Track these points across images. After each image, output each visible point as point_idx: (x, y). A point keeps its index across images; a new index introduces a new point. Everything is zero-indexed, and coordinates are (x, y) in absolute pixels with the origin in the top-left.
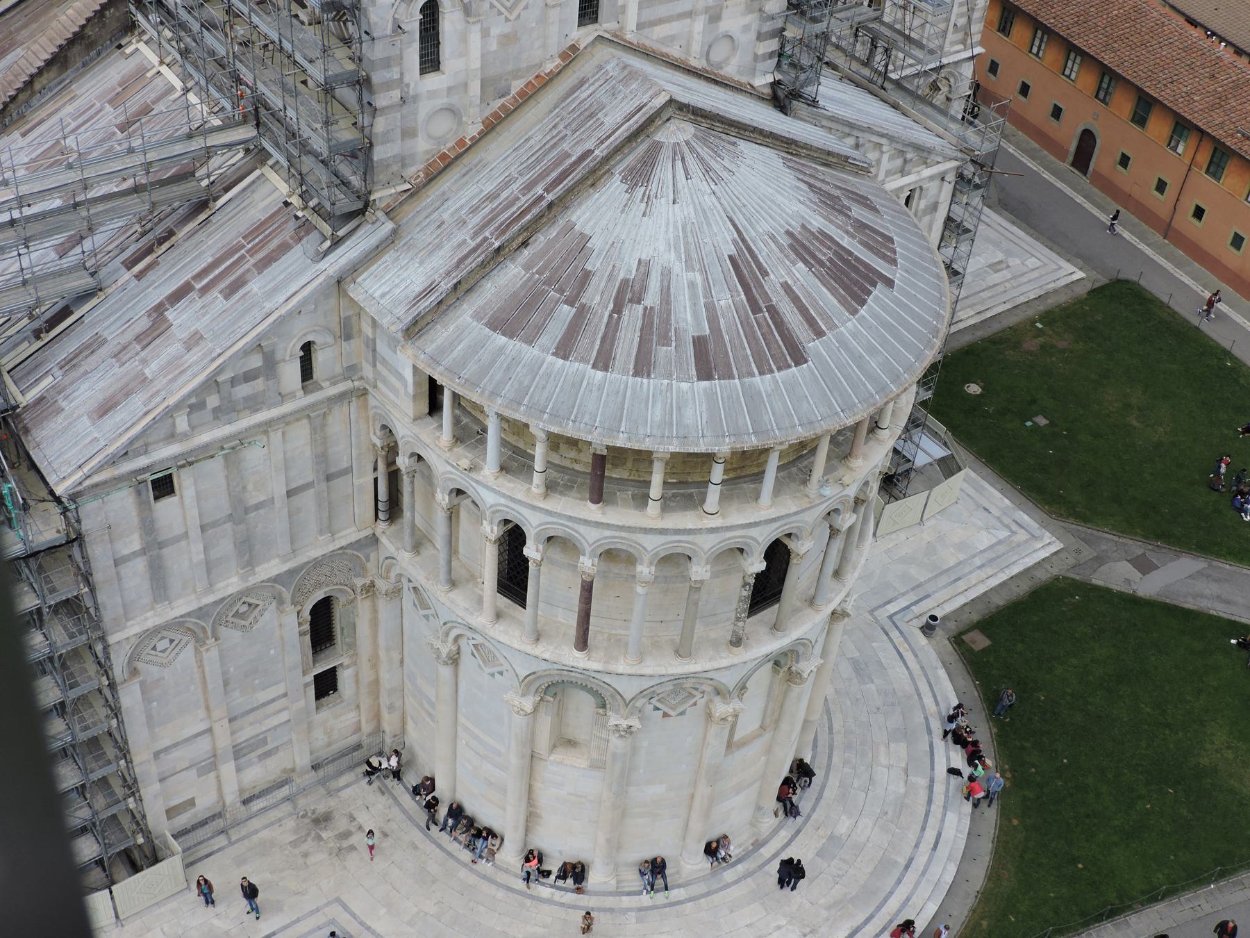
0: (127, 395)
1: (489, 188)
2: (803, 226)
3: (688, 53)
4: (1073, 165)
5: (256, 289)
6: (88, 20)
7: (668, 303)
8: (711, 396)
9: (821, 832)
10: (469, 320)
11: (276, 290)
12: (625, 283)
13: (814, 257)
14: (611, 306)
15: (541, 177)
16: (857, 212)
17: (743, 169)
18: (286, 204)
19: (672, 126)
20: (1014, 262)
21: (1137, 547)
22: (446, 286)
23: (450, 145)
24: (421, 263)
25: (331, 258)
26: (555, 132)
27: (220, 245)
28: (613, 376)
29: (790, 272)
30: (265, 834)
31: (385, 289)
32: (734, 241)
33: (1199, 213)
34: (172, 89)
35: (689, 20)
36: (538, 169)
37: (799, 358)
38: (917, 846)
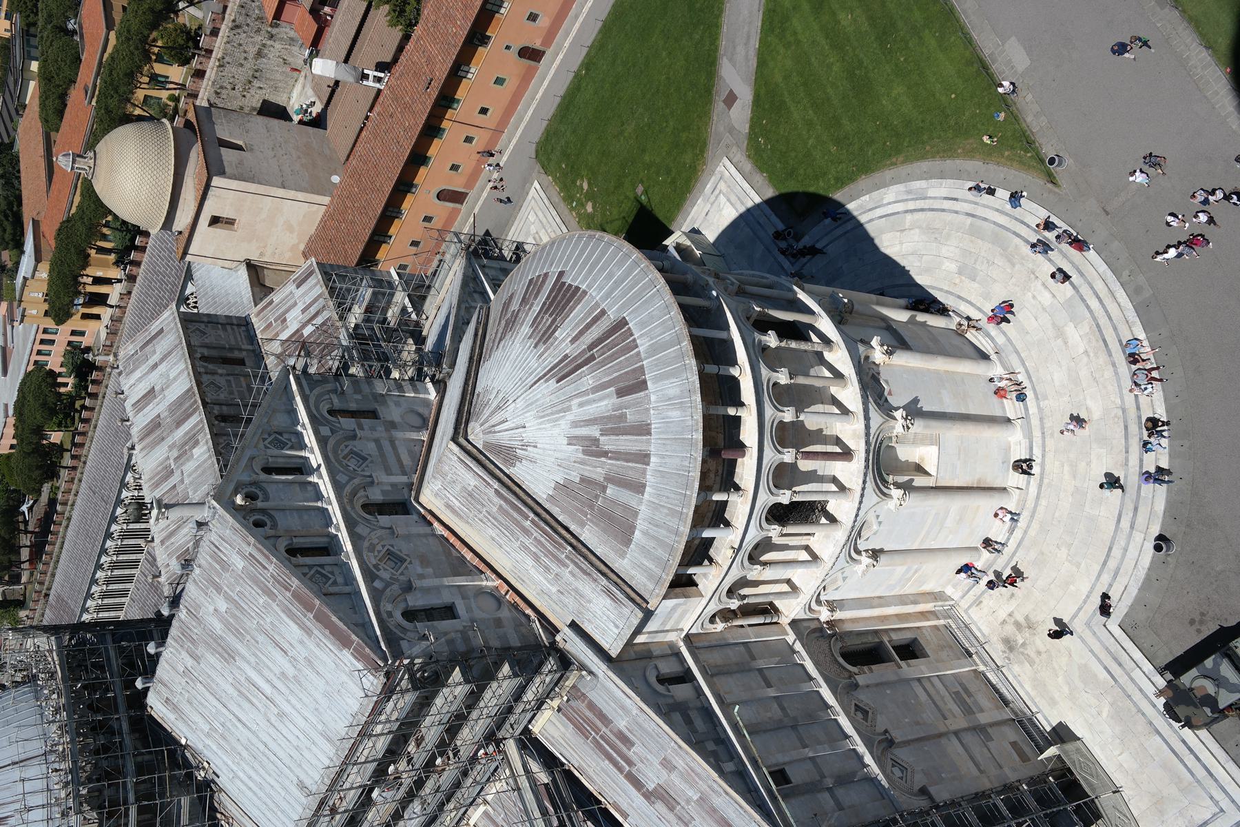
0: (714, 810)
1: (530, 562)
4: (462, 204)
5: (624, 723)
7: (596, 419)
8: (658, 379)
9: (957, 281)
11: (623, 708)
13: (550, 326)
14: (603, 459)
15: (518, 524)
16: (515, 306)
17: (495, 384)
18: (559, 710)
21: (719, 106)
22: (604, 581)
24: (590, 602)
25: (594, 669)
26: (485, 520)
27: (595, 756)
28: (653, 449)
29: (563, 340)
30: (1028, 687)
31: (611, 626)
32: (547, 381)
33: (484, 111)
34: (486, 813)
36: (513, 527)
37: (623, 323)
38: (956, 212)
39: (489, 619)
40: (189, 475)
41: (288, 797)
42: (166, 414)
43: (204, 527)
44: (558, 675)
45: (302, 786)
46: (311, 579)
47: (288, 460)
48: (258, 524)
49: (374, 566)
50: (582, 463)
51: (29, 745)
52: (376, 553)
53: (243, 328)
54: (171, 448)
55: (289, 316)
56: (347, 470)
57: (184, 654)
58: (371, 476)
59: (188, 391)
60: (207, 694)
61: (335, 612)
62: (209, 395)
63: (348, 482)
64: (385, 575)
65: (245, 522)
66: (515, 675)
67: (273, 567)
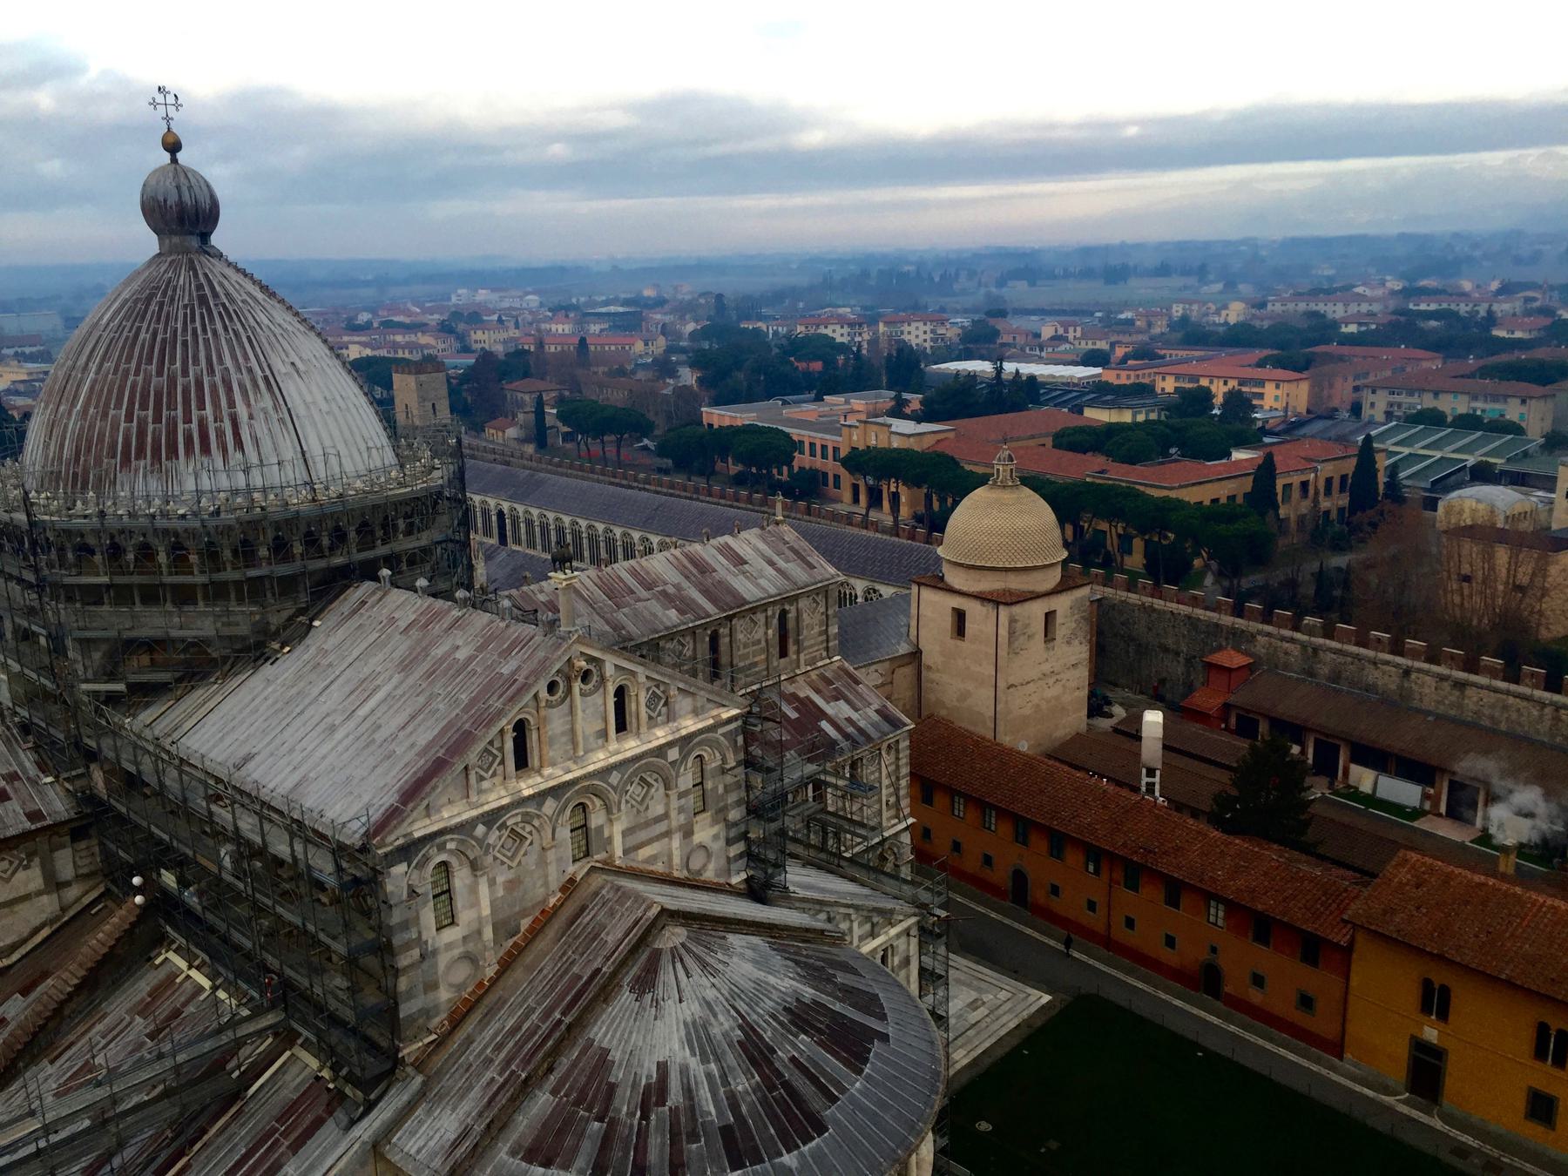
2: (798, 1000)
3: (671, 866)
7: (691, 1098)
10: (505, 1157)
12: (648, 1086)
14: (639, 1113)
16: (841, 978)
18: (318, 1078)
19: (666, 933)
20: (987, 997)
22: (479, 1128)
23: (470, 990)
24: (453, 1110)
25: (365, 1123)
32: (740, 1027)
33: (1130, 923)
34: (201, 989)
37: (821, 1128)
39: (436, 973)
45: (248, 758)
47: (634, 715)
48: (552, 687)
49: (505, 822)
50: (635, 1085)
51: (321, 466)
52: (521, 825)
53: (824, 654)
54: (678, 587)
55: (842, 703)
56: (625, 784)
62: (741, 622)
63: (609, 784)
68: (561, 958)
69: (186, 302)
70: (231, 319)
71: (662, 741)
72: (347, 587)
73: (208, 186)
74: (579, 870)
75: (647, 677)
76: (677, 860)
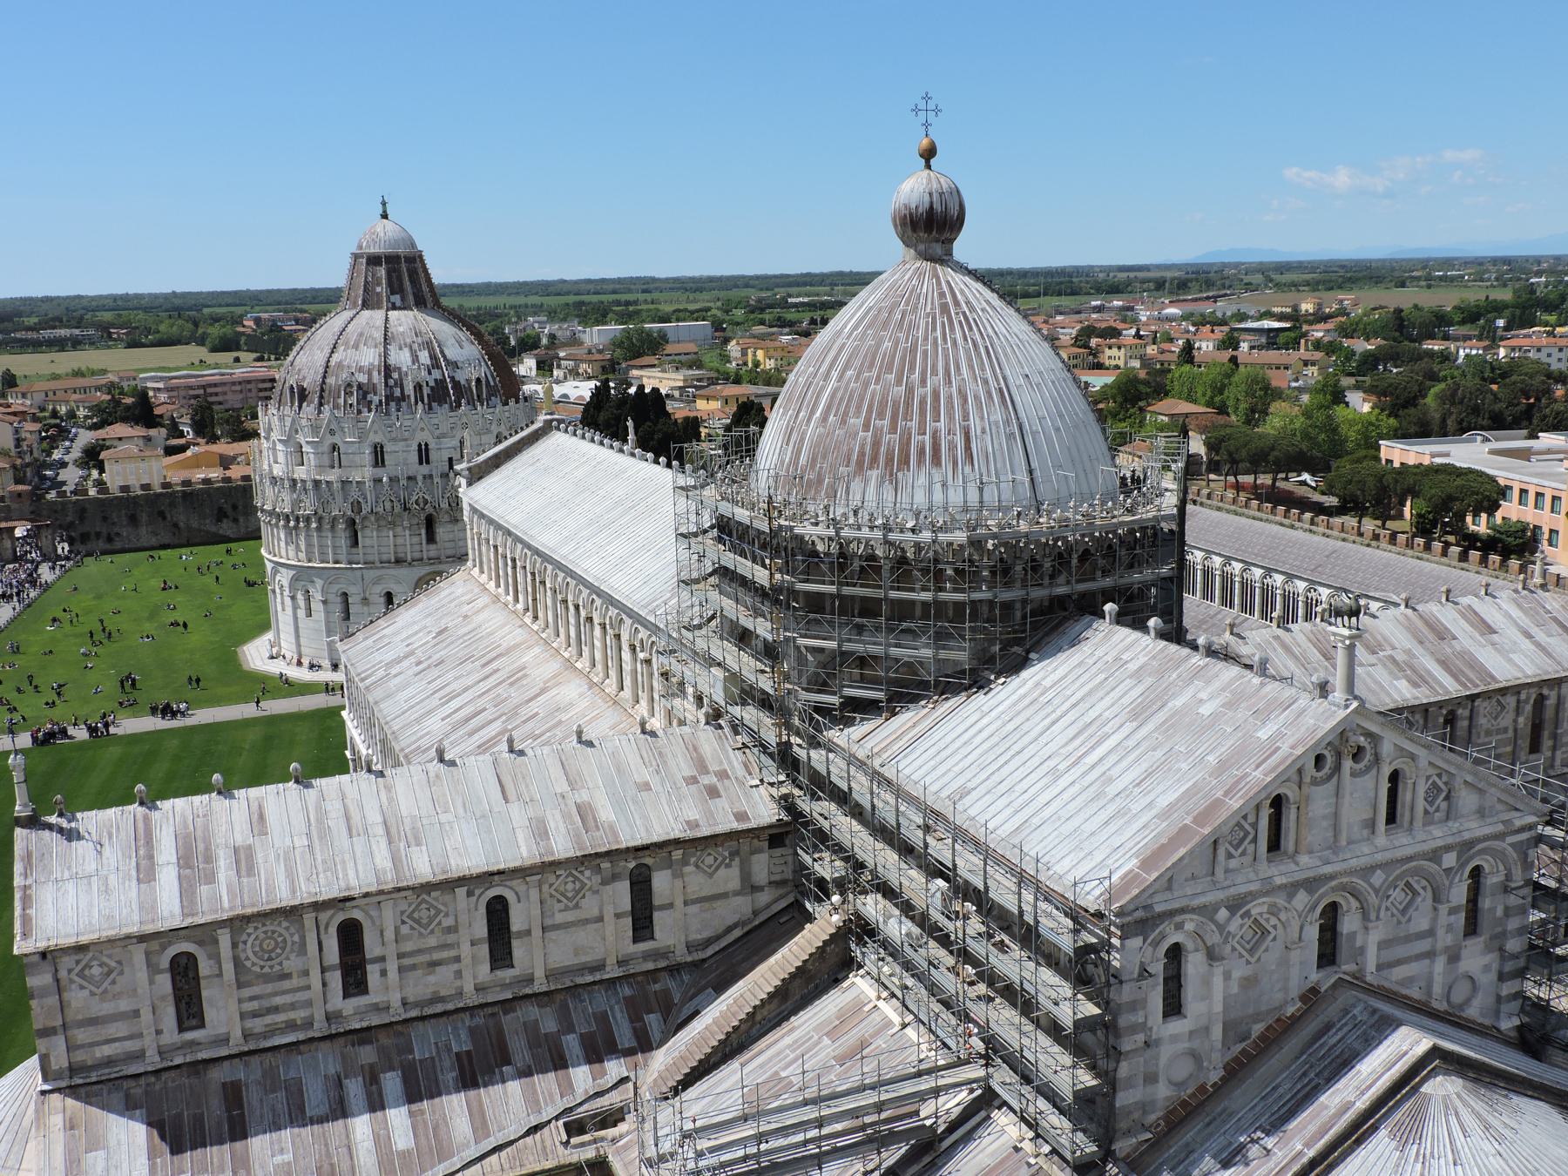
3: (1429, 993)
6: (811, 955)
18: (1017, 1149)
23: (1189, 1091)
34: (890, 1024)
35: (1427, 961)
39: (1157, 1065)
40: (1369, 674)
41: (951, 775)
42: (1458, 648)
43: (1317, 692)
44: (1068, 1156)
45: (964, 793)
46: (1238, 824)
48: (1319, 759)
49: (1249, 911)
52: (1265, 916)
54: (1408, 652)
56: (1388, 888)
57: (1142, 660)
58: (1378, 918)
59: (1493, 677)
60: (1090, 685)
61: (1191, 852)
63: (1371, 885)
64: (1233, 926)
65: (1324, 744)
66: (1076, 1094)
67: (1258, 776)
68: (1300, 1078)
69: (928, 310)
70: (971, 329)
71: (1440, 843)
72: (1066, 619)
73: (958, 191)
74: (1326, 979)
75: (1430, 763)
76: (1437, 989)
